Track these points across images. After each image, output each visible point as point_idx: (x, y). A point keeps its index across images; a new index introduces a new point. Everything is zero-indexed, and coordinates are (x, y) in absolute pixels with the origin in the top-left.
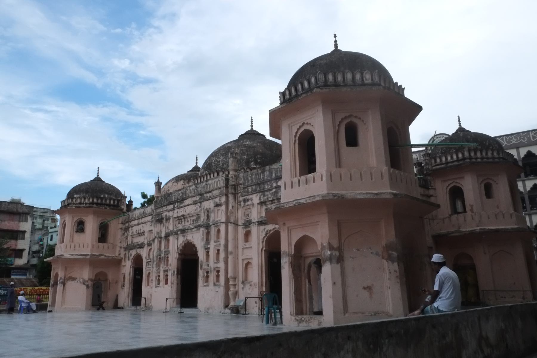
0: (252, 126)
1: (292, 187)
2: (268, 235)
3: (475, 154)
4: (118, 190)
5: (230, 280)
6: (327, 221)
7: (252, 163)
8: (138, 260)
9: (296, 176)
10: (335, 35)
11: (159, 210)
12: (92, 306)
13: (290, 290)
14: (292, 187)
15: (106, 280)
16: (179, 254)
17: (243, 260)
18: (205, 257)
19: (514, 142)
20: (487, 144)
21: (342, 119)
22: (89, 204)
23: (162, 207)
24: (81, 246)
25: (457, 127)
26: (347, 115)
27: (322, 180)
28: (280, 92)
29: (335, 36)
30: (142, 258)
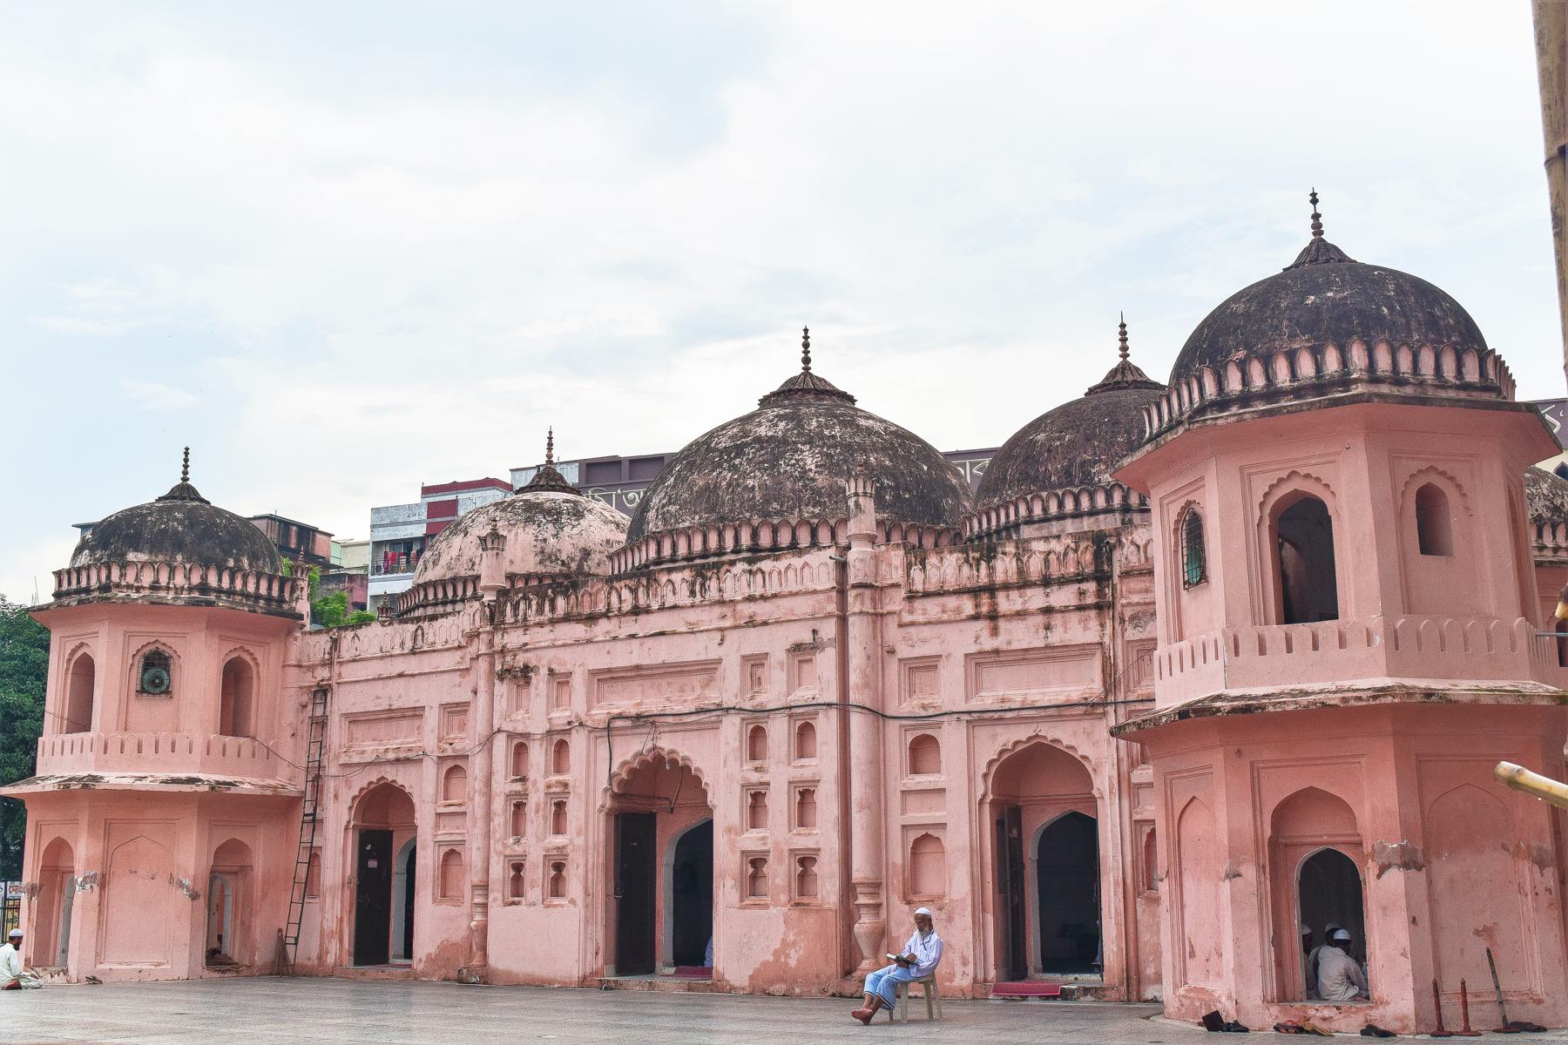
0: (806, 360)
1: (1262, 651)
2: (1005, 756)
3: (1540, 536)
5: (859, 890)
6: (1391, 753)
10: (1314, 195)
11: (514, 639)
12: (208, 964)
13: (1262, 935)
15: (244, 870)
16: (615, 796)
18: (747, 812)
22: (190, 589)
23: (526, 628)
24: (165, 746)
26: (1424, 466)
29: (1314, 201)
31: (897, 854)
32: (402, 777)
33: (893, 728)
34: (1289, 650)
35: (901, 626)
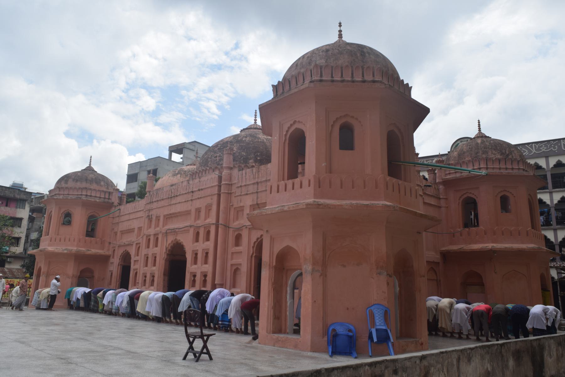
1: (278, 192)
4: (112, 182)
7: (251, 161)
8: (126, 257)
9: (283, 180)
10: (340, 23)
14: (278, 192)
16: (168, 255)
17: (232, 265)
19: (544, 150)
20: (507, 152)
21: (337, 119)
25: (477, 132)
27: (309, 186)
28: (273, 86)
29: (340, 25)
30: (130, 255)
31: (229, 274)
32: (128, 249)
33: (231, 230)
34: (286, 190)
35: (235, 197)
